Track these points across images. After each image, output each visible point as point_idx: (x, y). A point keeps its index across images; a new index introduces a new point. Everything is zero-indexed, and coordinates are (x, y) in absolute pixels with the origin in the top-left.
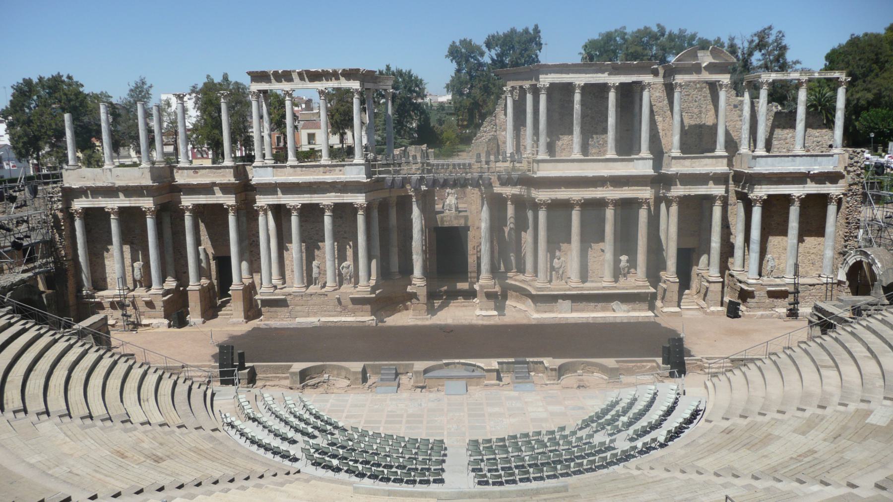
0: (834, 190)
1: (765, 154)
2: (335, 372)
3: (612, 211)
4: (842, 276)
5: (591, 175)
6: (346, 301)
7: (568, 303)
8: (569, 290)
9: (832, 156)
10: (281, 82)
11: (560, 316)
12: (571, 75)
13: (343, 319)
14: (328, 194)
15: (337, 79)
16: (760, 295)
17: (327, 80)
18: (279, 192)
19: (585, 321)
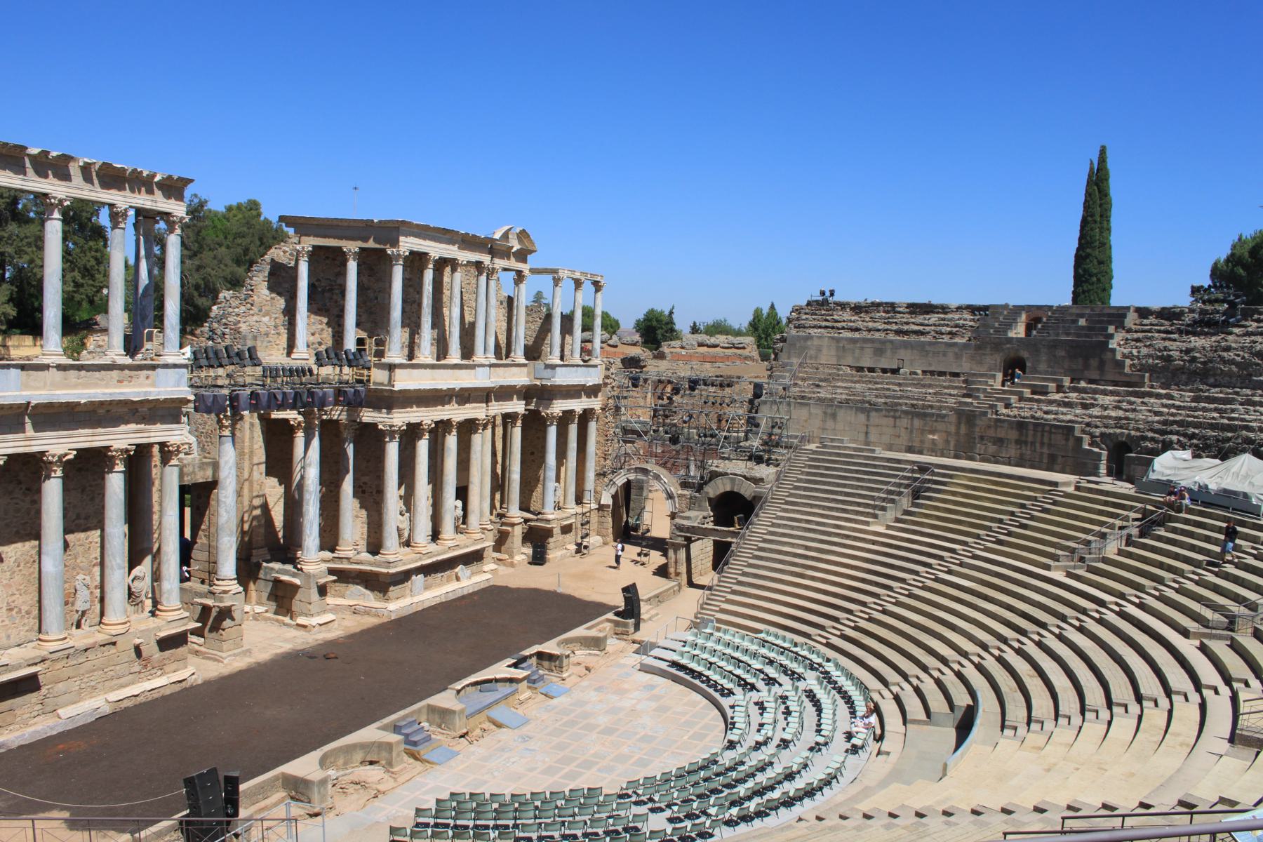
0: (596, 403)
1: (560, 362)
2: (341, 762)
3: (455, 439)
4: (607, 499)
5: (445, 388)
6: (151, 649)
7: (418, 579)
8: (420, 559)
9: (595, 366)
10: (46, 177)
11: (416, 599)
12: (428, 243)
13: (148, 685)
14: (123, 428)
15: (150, 192)
16: (557, 531)
17: (133, 191)
18: (29, 426)
19: (438, 601)
